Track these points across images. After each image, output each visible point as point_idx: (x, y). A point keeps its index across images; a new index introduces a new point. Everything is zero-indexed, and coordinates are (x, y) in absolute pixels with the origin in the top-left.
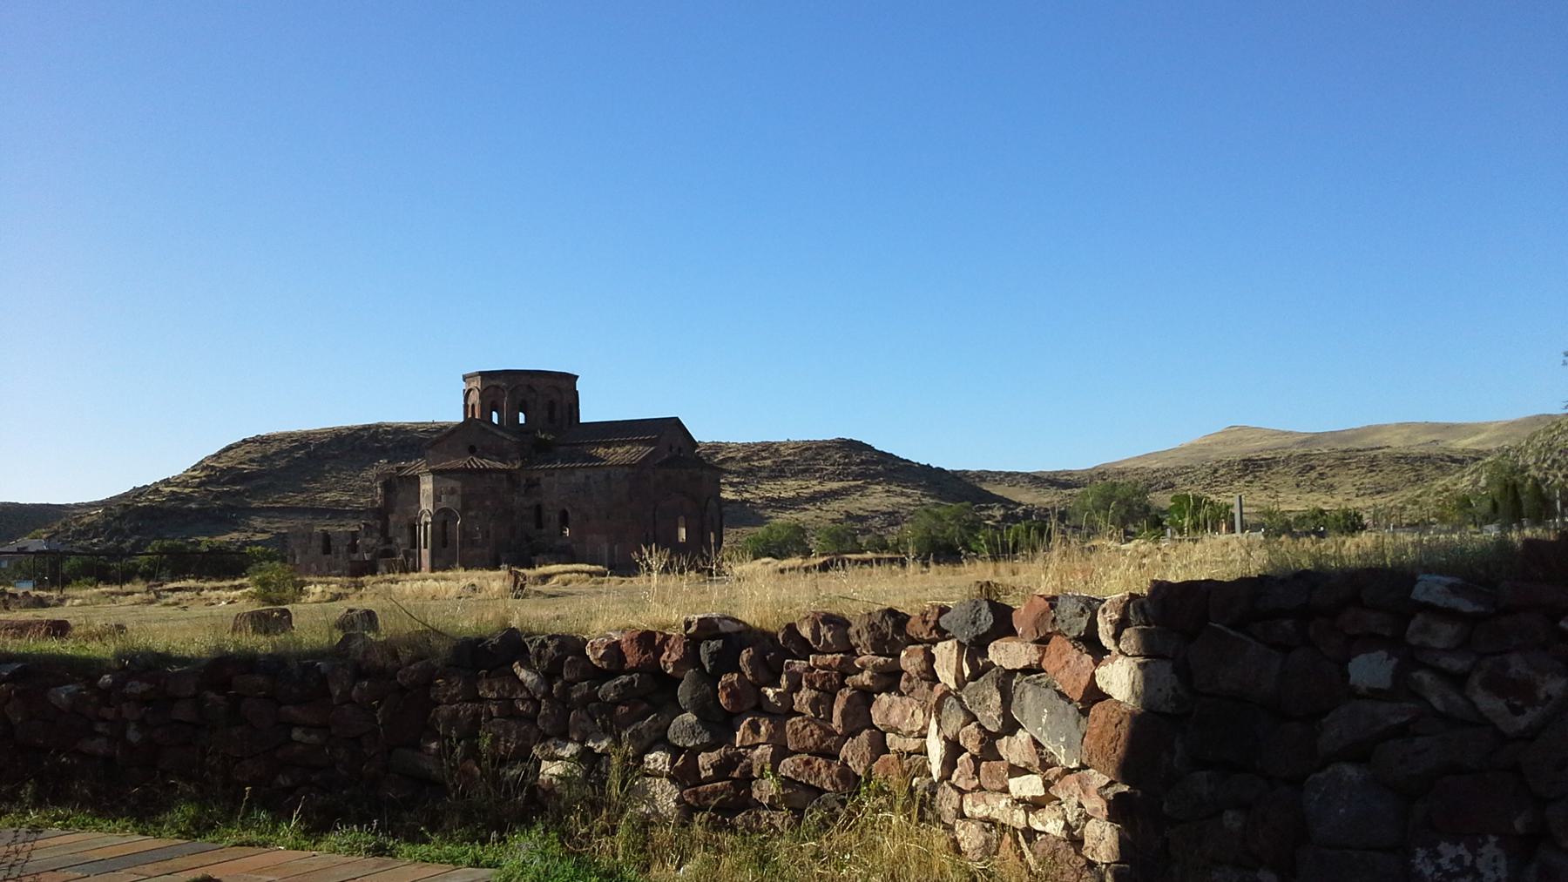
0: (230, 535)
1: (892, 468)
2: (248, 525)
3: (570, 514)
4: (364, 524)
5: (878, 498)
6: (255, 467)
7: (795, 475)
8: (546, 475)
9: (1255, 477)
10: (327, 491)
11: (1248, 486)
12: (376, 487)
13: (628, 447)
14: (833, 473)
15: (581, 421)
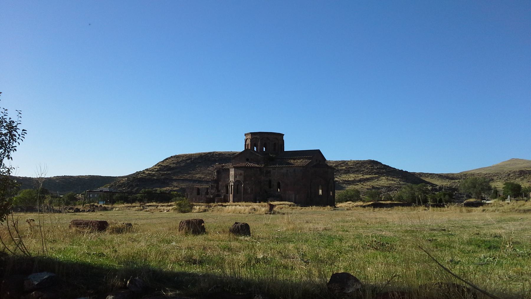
0: (166, 188)
1: (389, 171)
2: (172, 185)
3: (281, 184)
4: (211, 185)
5: (383, 181)
6: (175, 165)
7: (353, 172)
8: (273, 169)
9: (525, 177)
10: (197, 174)
11: (522, 181)
12: (215, 172)
13: (301, 160)
14: (367, 172)
15: (285, 151)
